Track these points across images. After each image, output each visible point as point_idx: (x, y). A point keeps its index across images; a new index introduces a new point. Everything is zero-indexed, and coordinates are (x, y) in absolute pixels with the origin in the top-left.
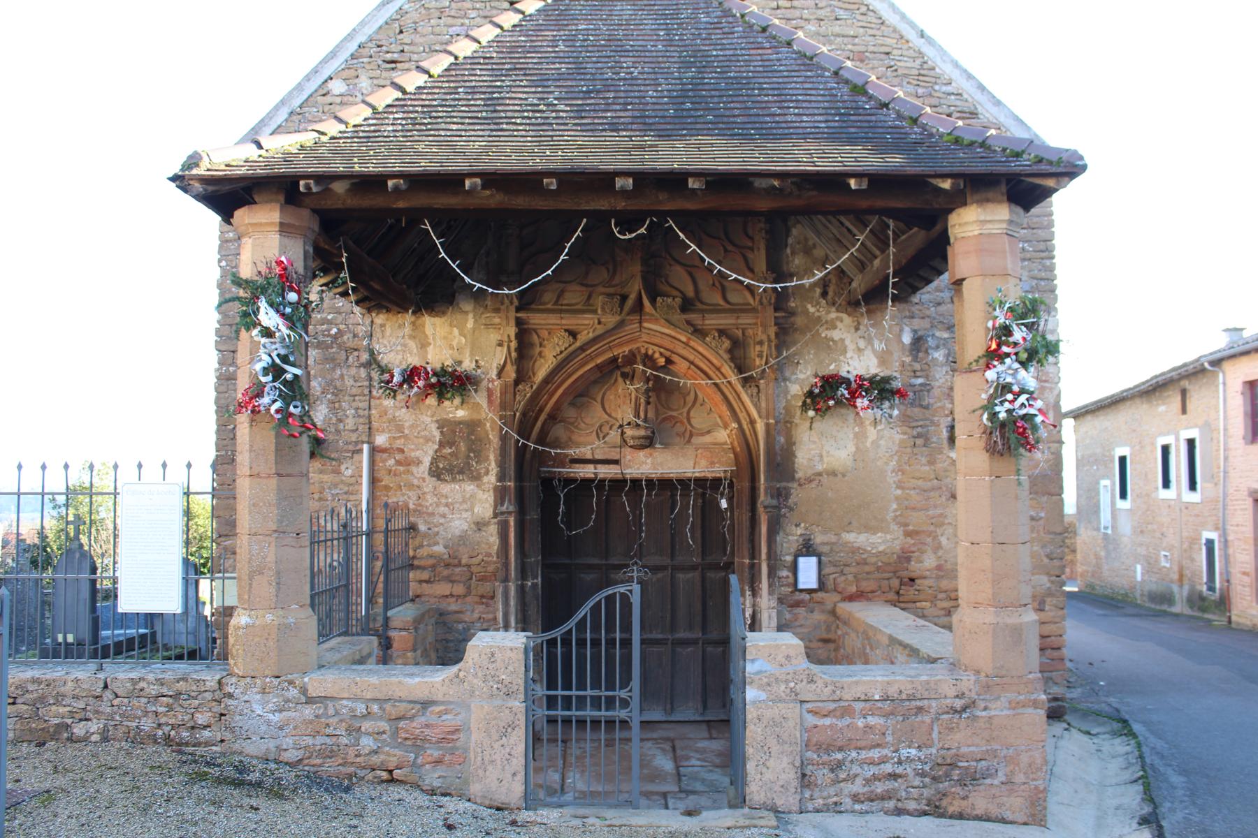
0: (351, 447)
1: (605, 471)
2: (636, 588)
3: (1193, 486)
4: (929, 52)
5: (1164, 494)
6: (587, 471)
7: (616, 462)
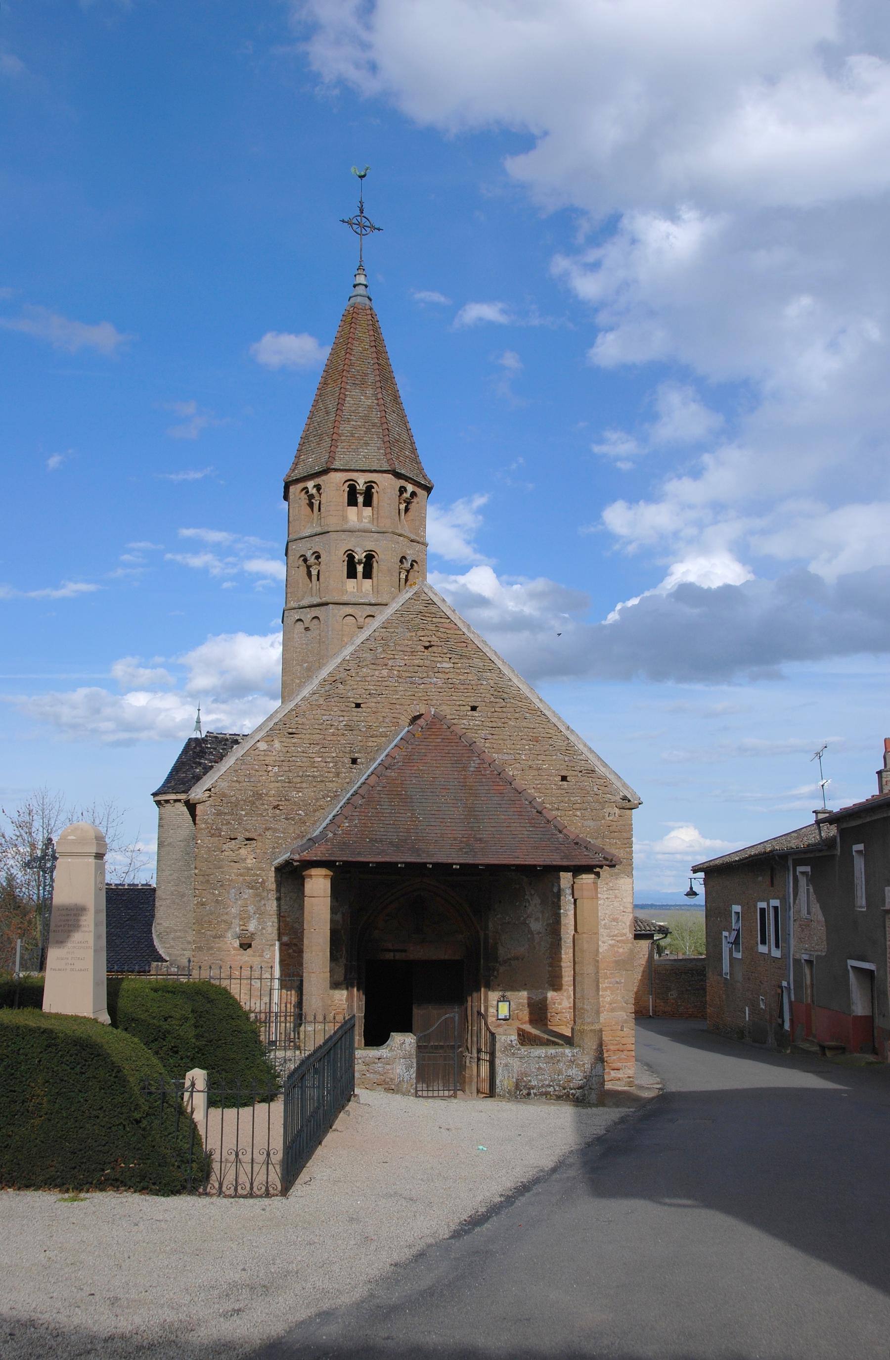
0: (269, 943)
1: (399, 956)
2: (457, 1015)
3: (777, 946)
4: (572, 738)
5: (763, 949)
6: (390, 956)
7: (405, 951)
